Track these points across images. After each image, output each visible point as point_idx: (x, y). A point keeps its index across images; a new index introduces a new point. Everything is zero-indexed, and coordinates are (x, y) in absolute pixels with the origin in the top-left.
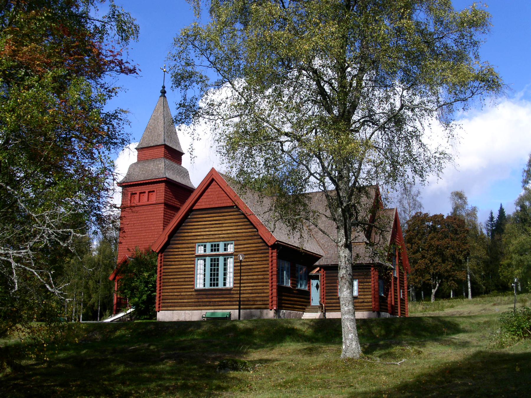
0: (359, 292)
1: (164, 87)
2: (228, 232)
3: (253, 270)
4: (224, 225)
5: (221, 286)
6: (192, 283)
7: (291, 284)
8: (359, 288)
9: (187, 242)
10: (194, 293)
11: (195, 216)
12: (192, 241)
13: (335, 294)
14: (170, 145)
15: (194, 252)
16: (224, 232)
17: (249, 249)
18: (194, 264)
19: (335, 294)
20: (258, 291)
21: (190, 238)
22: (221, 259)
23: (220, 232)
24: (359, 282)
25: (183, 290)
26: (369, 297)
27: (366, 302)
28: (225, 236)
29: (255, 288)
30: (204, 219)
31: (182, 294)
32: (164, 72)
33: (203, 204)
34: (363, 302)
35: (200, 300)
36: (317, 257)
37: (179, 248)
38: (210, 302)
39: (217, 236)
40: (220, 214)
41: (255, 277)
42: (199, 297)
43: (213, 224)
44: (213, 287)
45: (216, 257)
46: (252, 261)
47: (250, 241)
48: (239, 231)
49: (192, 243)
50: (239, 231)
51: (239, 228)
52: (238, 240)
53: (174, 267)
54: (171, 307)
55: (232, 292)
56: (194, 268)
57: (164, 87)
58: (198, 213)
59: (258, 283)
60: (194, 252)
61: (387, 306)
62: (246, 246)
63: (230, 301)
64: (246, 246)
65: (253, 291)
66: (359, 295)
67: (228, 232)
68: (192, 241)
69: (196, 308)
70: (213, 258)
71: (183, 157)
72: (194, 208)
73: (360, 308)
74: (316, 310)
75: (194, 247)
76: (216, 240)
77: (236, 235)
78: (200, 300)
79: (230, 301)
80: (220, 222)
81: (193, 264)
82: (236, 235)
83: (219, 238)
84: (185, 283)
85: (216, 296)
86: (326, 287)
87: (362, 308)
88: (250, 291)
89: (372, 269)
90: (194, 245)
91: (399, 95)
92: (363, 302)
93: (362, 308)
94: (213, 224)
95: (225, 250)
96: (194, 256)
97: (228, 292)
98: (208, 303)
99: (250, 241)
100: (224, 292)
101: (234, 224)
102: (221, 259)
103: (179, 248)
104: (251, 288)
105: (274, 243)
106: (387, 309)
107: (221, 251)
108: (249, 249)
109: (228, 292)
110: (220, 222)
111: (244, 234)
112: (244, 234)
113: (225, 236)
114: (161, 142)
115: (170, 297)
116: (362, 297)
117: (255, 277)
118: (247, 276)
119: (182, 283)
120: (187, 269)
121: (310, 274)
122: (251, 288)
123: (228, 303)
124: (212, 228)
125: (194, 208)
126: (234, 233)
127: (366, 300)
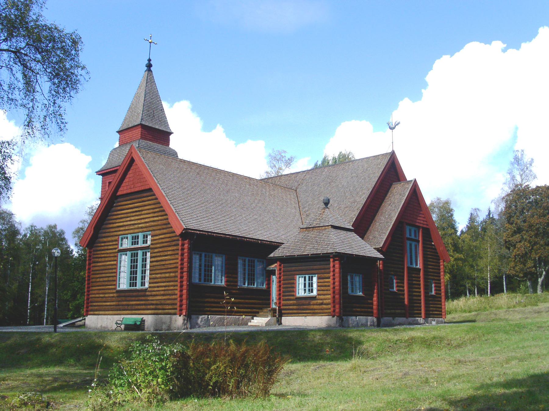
0: (318, 290)
1: (149, 60)
2: (147, 220)
3: (166, 267)
4: (143, 212)
5: (139, 287)
6: (114, 283)
7: (226, 282)
8: (318, 286)
9: (112, 234)
10: (115, 295)
11: (120, 204)
12: (116, 233)
13: (292, 293)
14: (150, 125)
15: (116, 247)
16: (143, 221)
17: (163, 240)
18: (116, 260)
19: (292, 293)
20: (170, 292)
21: (114, 230)
22: (140, 253)
23: (139, 221)
24: (319, 278)
25: (107, 291)
26: (328, 298)
27: (325, 304)
28: (143, 225)
29: (167, 288)
30: (127, 207)
31: (106, 295)
32: (150, 43)
33: (125, 188)
34: (322, 304)
35: (120, 303)
36: (274, 246)
37: (105, 242)
38: (128, 305)
39: (136, 226)
40: (140, 200)
41: (167, 275)
42: (120, 299)
43: (136, 211)
44: (132, 288)
45: (136, 252)
46: (166, 256)
47: (165, 231)
48: (155, 219)
49: (116, 236)
50: (155, 219)
51: (155, 215)
52: (154, 230)
53: (100, 264)
54: (97, 310)
55: (147, 293)
56: (116, 265)
57: (149, 60)
58: (122, 199)
59: (170, 282)
60: (116, 247)
61: (372, 308)
62: (161, 237)
63: (144, 305)
64: (161, 237)
65: (166, 292)
66: (318, 295)
67: (147, 220)
68: (116, 233)
69: (116, 312)
70: (133, 252)
71: (171, 137)
72: (119, 193)
73: (319, 311)
74: (267, 314)
75: (117, 240)
76: (136, 231)
77: (152, 224)
78: (120, 303)
79: (144, 305)
80: (140, 209)
81: (115, 260)
82: (152, 224)
83: (138, 228)
84: (109, 283)
85: (133, 298)
86: (283, 284)
87: (321, 311)
88: (162, 293)
89: (331, 260)
90: (117, 238)
91: (31, 13)
92: (322, 304)
93: (321, 311)
94: (136, 211)
95: (145, 242)
96: (117, 250)
97: (143, 293)
98: (126, 307)
99: (165, 231)
100: (140, 293)
101: (152, 211)
102: (140, 253)
103: (105, 242)
104: (163, 289)
105: (182, 232)
106: (372, 312)
107: (140, 245)
108: (163, 240)
109: (143, 293)
110: (140, 209)
111: (159, 223)
112: (159, 223)
113: (143, 225)
114: (138, 122)
115: (96, 299)
116: (322, 297)
117: (167, 275)
118: (161, 273)
119: (106, 283)
120: (111, 267)
121: (268, 269)
122: (163, 289)
123: (143, 307)
124: (133, 216)
125: (119, 193)
126: (151, 222)
127: (325, 301)
